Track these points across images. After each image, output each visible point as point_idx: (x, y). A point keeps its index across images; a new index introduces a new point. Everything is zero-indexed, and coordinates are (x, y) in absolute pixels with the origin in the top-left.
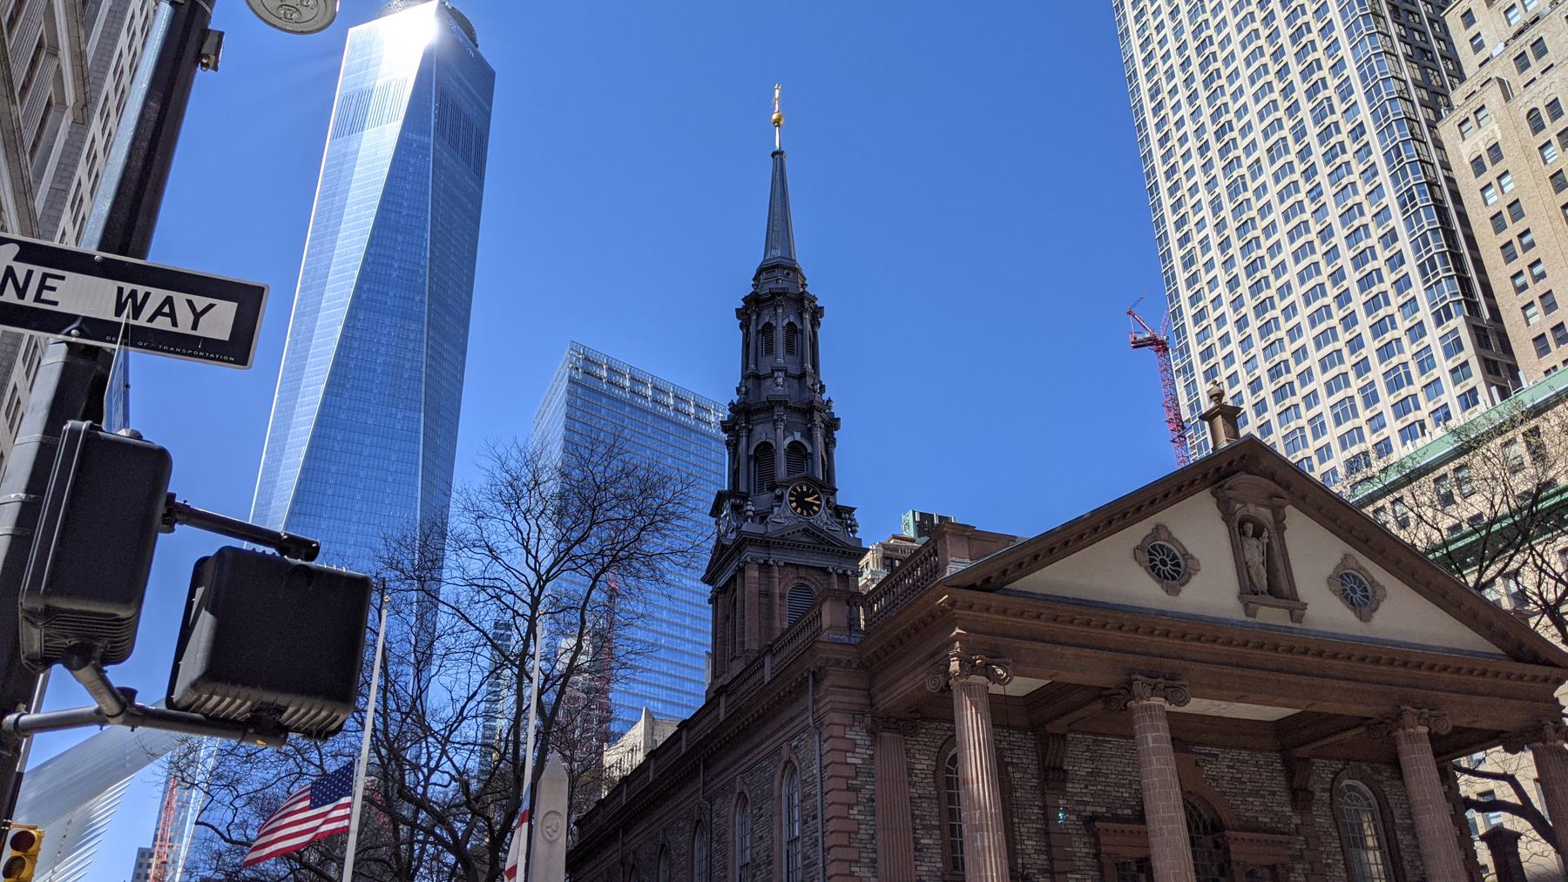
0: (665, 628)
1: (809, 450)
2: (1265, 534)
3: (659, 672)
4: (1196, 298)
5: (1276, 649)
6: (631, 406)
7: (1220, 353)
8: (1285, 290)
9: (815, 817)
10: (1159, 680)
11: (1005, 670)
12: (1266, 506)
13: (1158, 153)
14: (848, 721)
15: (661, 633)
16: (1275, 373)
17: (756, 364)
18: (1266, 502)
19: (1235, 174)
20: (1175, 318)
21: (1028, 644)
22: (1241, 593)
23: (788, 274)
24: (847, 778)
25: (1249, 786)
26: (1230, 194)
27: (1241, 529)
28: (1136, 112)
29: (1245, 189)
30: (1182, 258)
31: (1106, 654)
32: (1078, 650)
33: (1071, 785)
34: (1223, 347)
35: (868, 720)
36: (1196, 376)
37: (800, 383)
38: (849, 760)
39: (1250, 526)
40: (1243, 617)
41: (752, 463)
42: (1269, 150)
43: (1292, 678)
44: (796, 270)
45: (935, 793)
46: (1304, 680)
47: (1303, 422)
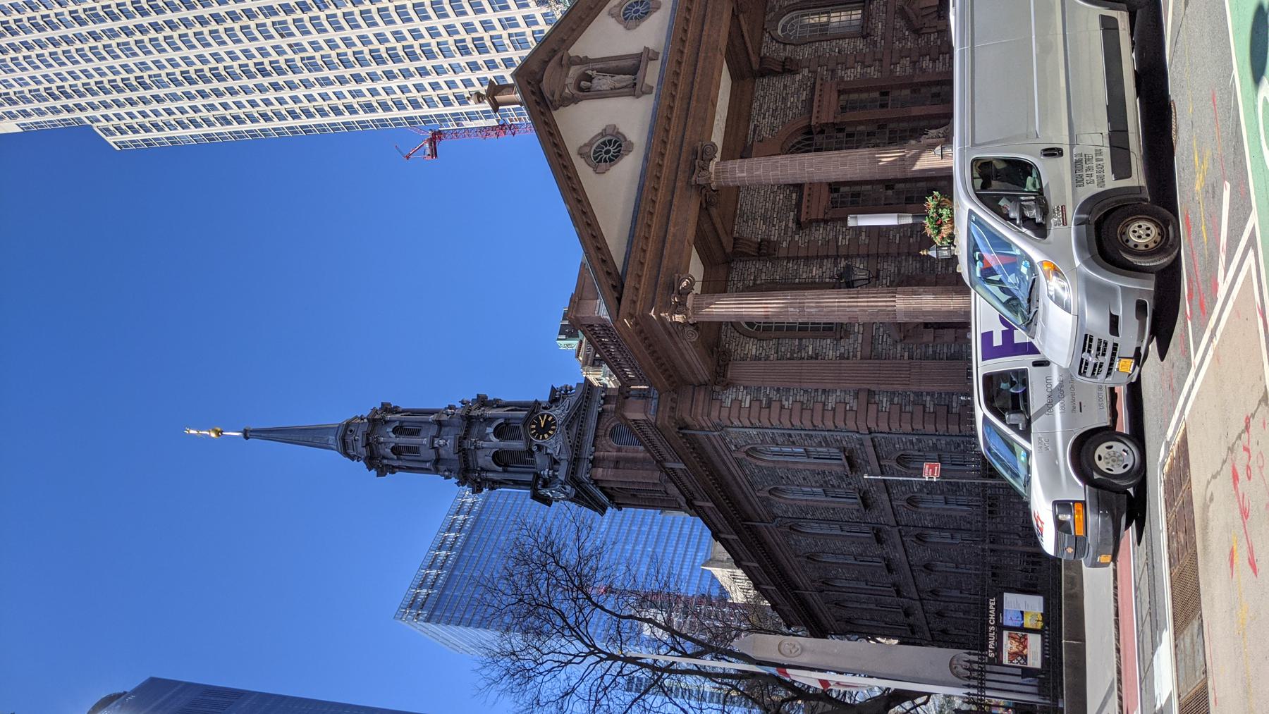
0: (639, 548)
1: (502, 421)
2: (590, 72)
3: (674, 554)
4: (400, 105)
5: (678, 74)
6: (454, 569)
7: (445, 90)
8: (398, 36)
9: (790, 435)
10: (697, 164)
11: (683, 280)
12: (569, 68)
13: (276, 123)
14: (718, 403)
15: (643, 551)
16: (464, 51)
17: (426, 462)
18: (565, 69)
19: (300, 64)
20: (415, 123)
21: (665, 262)
22: (634, 95)
23: (351, 431)
24: (761, 408)
26: (316, 70)
27: (585, 90)
28: (239, 137)
29: (313, 58)
30: (365, 112)
31: (675, 202)
32: (671, 223)
34: (441, 88)
35: (717, 388)
36: (463, 111)
37: (446, 426)
38: (747, 405)
39: (582, 83)
40: (652, 97)
41: (509, 469)
42: (282, 36)
43: (700, 64)
44: (348, 425)
46: (702, 55)
47: (505, 34)
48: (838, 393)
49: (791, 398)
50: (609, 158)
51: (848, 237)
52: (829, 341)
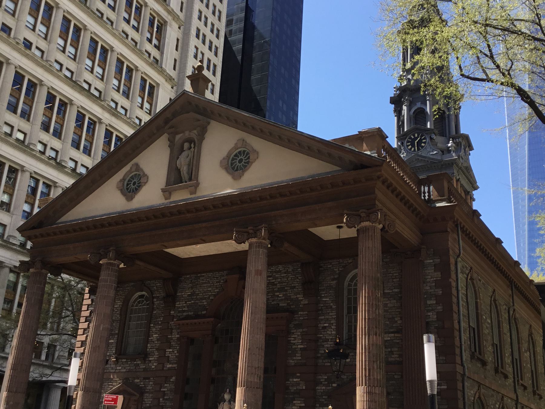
25: (278, 286)
33: (178, 303)
45: (120, 317)
50: (137, 186)
51: (170, 355)
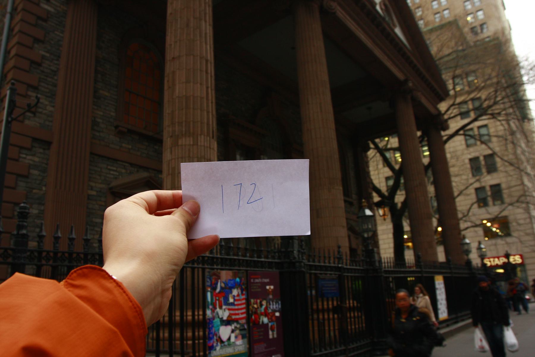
48: (52, 109)
49: (48, 55)
52: (113, 114)
